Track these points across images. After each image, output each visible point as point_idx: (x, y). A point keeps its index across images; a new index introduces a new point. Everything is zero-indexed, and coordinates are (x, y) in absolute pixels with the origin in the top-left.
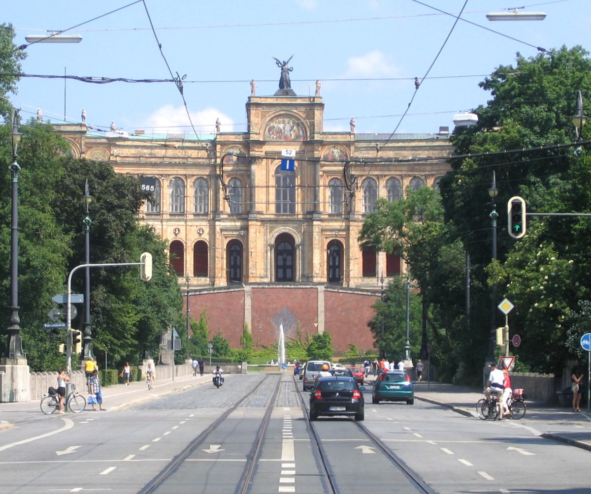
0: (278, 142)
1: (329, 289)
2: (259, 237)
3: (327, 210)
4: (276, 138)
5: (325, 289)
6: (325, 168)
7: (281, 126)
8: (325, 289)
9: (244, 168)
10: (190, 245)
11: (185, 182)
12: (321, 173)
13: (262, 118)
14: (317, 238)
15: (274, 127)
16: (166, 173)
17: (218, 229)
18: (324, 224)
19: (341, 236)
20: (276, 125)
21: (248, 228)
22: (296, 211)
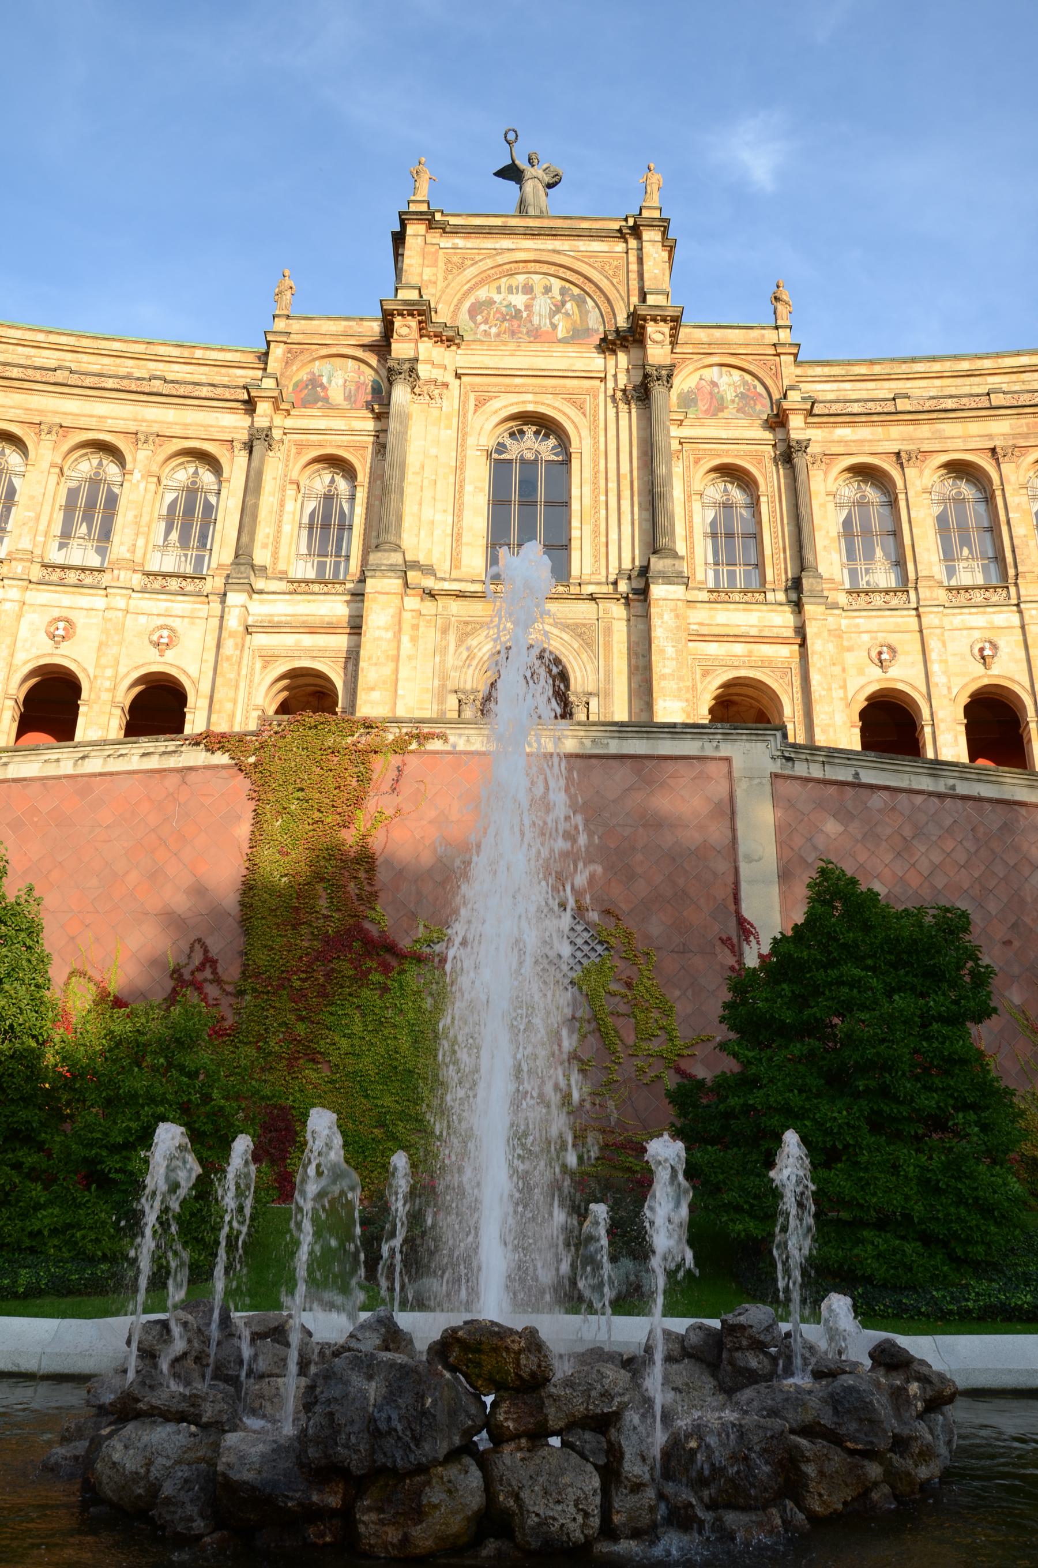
0: (504, 343)
1: (800, 769)
2: (410, 658)
3: (700, 576)
4: (498, 335)
5: (776, 767)
6: (685, 432)
7: (519, 300)
8: (776, 767)
9: (370, 425)
10: (108, 684)
11: (128, 458)
12: (675, 445)
13: (448, 271)
14: (670, 651)
15: (491, 302)
16: (58, 421)
17: (233, 622)
18: (699, 616)
19: (766, 664)
20: (497, 298)
21: (361, 627)
22: (575, 571)
